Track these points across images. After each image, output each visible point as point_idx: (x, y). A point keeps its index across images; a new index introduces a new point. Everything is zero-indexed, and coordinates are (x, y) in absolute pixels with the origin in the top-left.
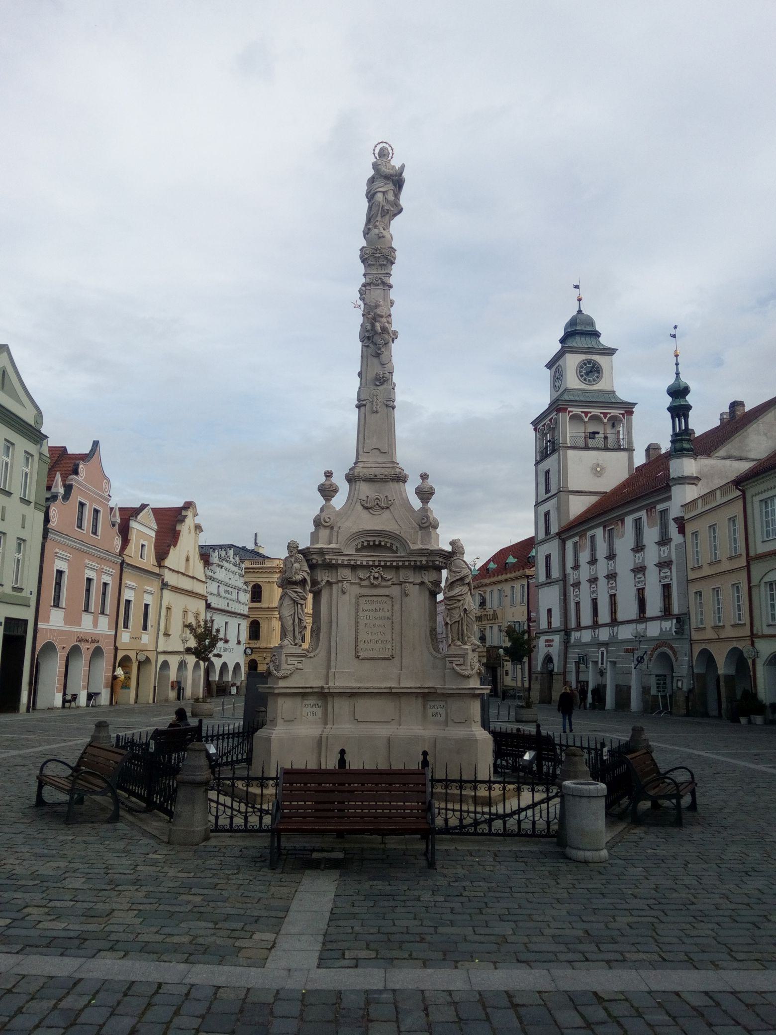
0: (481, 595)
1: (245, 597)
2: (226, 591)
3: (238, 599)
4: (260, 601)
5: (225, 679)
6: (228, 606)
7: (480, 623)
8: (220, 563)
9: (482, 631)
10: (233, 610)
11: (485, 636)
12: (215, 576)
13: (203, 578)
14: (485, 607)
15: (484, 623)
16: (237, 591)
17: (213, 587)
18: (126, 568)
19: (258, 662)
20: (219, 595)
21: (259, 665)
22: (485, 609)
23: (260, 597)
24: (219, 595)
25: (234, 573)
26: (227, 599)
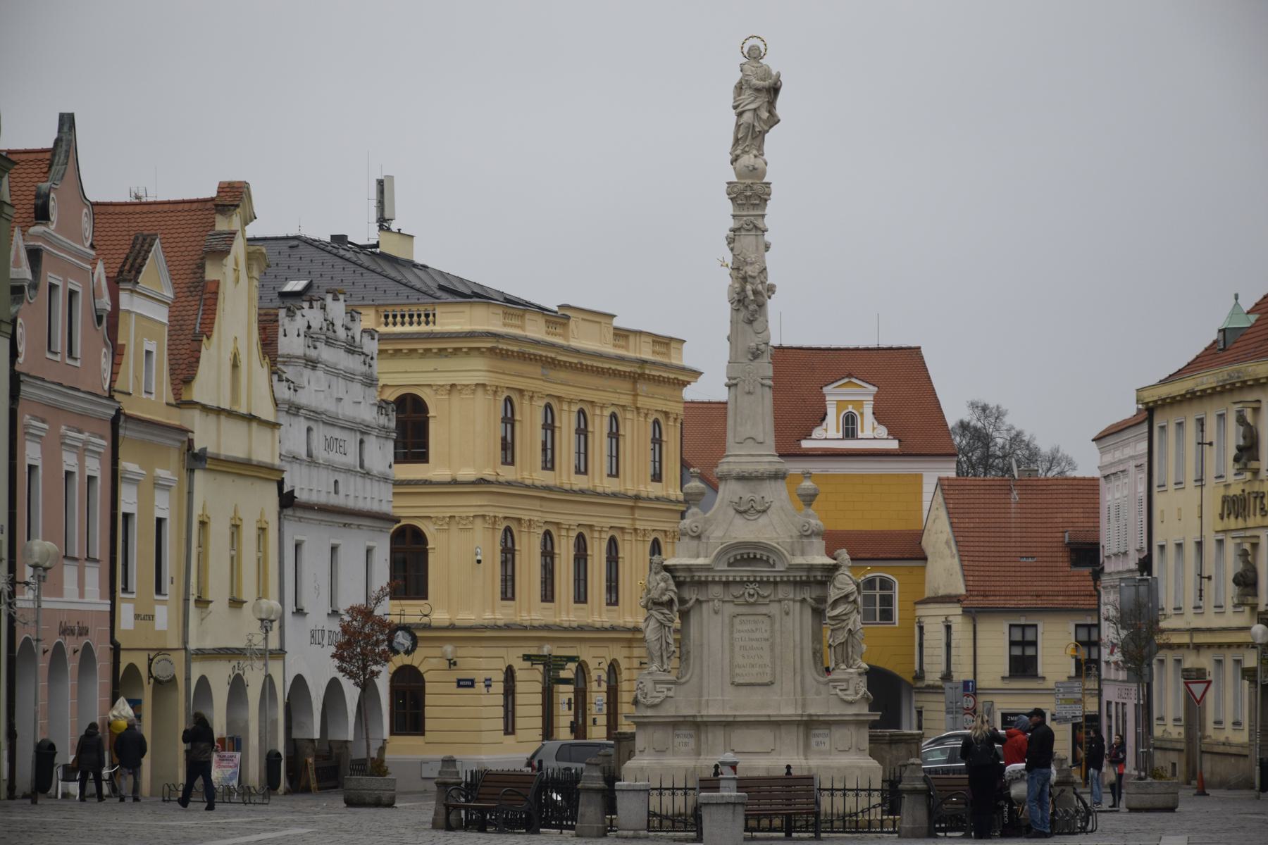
0: (1241, 420)
1: (380, 454)
2: (330, 444)
3: (362, 466)
4: (423, 457)
5: (336, 735)
6: (336, 492)
7: (1240, 523)
8: (312, 353)
9: (1244, 554)
10: (351, 504)
11: (1254, 571)
12: (302, 398)
13: (266, 411)
14: (1254, 465)
15: (1251, 522)
16: (359, 436)
17: (294, 436)
18: (126, 428)
19: (427, 677)
20: (311, 460)
21: (429, 688)
22: (1256, 472)
23: (425, 445)
24: (311, 460)
25: (349, 376)
26: (335, 469)
